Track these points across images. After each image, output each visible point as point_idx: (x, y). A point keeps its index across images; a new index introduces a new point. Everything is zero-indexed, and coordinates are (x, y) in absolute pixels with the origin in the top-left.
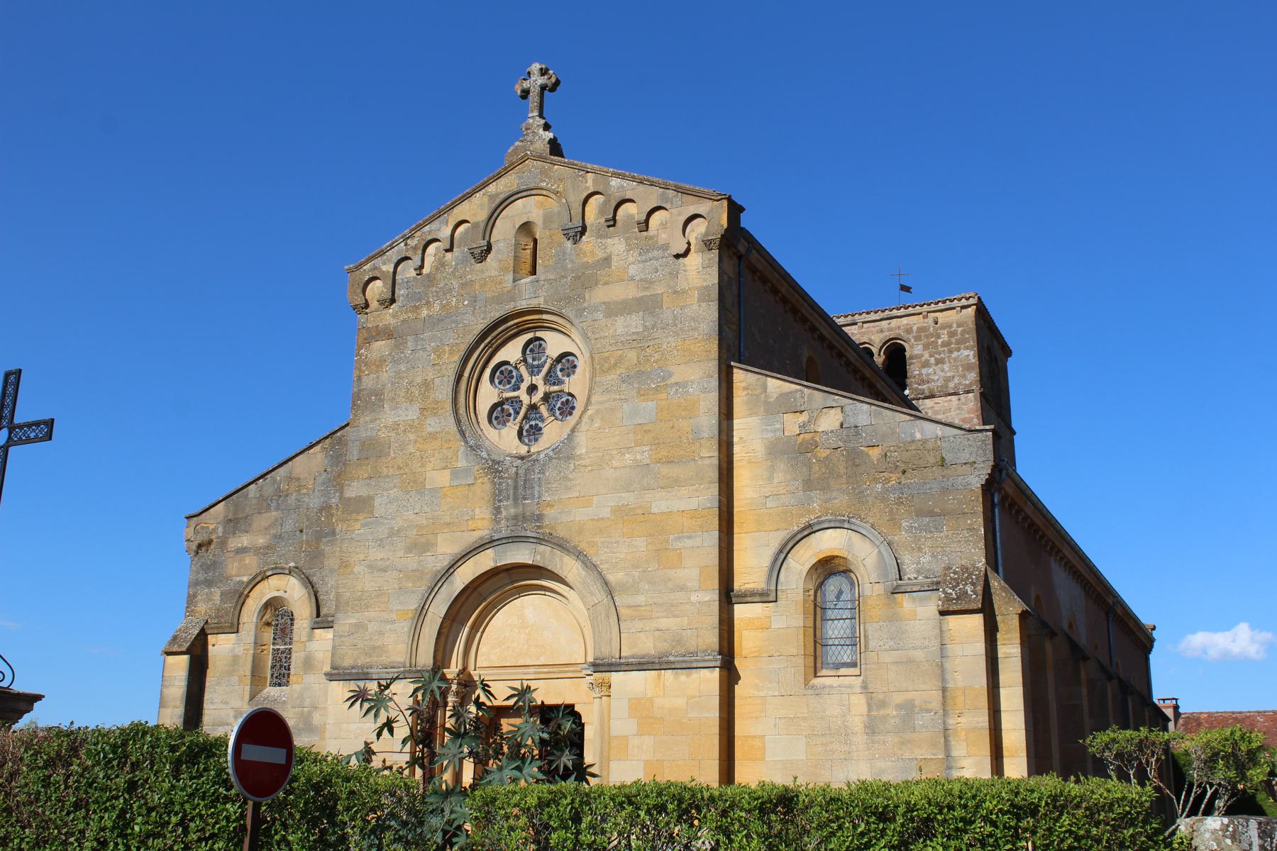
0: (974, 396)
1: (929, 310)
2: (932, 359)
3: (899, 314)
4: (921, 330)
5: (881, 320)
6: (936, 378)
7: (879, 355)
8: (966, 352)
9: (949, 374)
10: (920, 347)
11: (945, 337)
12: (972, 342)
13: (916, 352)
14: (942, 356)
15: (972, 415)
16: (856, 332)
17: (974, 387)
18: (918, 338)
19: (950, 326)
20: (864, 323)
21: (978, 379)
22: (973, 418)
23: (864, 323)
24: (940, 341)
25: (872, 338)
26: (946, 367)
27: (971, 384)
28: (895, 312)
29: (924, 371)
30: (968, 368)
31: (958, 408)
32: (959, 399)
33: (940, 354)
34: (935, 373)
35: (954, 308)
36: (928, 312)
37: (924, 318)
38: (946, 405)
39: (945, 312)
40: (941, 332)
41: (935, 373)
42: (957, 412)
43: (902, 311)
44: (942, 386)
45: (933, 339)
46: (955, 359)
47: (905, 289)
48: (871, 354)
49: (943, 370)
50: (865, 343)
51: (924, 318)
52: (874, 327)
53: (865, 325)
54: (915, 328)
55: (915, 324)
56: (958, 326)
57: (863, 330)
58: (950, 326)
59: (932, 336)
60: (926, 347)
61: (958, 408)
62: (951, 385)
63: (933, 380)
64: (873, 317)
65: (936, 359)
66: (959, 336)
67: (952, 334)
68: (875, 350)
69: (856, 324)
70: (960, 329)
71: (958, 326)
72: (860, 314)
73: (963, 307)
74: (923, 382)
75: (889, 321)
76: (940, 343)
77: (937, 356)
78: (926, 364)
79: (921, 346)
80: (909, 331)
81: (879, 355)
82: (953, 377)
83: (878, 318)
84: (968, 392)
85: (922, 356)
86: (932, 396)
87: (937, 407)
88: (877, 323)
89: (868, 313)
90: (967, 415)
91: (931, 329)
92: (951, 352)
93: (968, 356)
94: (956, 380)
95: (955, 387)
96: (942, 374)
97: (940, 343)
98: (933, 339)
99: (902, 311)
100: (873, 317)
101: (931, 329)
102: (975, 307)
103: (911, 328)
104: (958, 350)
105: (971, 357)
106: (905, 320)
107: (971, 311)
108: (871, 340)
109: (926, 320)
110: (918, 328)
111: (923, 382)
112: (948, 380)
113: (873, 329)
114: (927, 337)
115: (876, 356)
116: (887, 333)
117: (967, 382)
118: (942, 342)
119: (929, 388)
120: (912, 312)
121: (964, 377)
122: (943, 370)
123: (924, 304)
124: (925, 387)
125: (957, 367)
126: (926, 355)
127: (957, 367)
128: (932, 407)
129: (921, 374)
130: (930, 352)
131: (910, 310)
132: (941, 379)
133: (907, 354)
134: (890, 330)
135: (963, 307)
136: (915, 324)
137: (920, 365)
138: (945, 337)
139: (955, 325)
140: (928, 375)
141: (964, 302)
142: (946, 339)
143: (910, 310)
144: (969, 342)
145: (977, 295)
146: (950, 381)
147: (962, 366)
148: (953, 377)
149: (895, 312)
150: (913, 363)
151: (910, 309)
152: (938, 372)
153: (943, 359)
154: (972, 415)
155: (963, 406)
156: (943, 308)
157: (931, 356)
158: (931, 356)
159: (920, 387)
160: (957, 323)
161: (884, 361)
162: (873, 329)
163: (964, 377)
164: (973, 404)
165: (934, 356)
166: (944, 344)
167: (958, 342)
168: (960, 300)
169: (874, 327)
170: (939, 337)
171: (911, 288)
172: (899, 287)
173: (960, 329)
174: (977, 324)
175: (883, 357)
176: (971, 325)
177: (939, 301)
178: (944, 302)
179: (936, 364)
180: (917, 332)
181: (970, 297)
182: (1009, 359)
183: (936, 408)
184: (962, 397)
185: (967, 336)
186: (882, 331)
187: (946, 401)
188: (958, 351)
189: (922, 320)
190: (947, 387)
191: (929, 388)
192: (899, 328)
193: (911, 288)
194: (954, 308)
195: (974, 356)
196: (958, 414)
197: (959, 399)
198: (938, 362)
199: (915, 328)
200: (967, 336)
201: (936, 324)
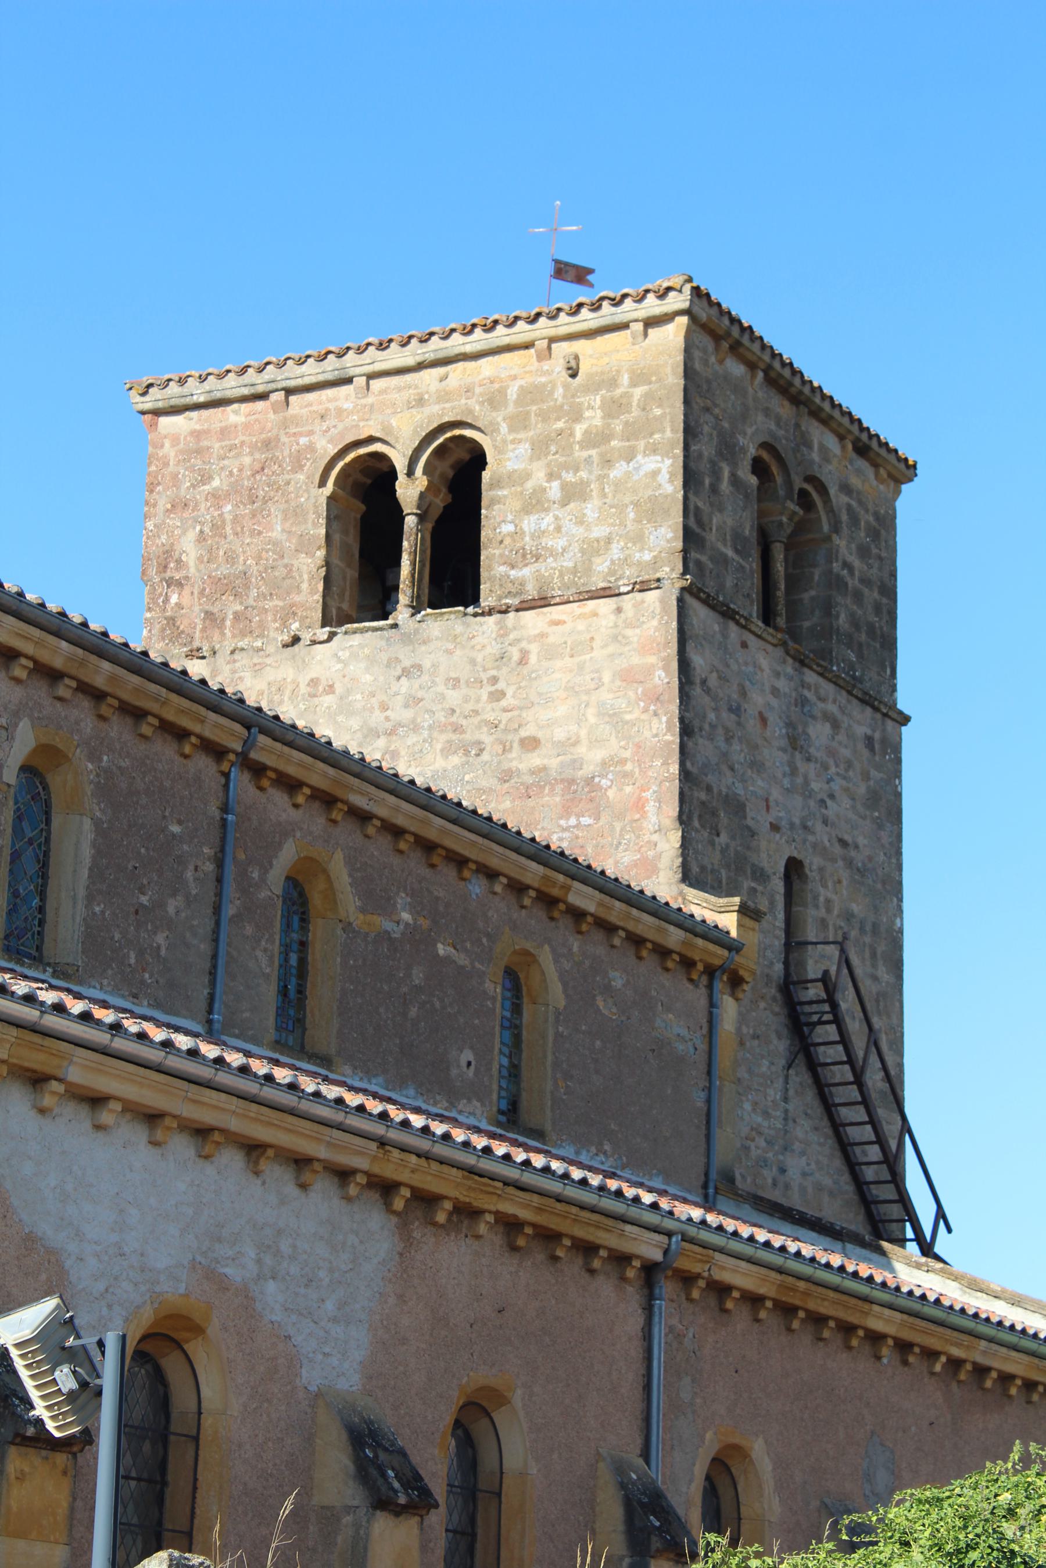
0: (662, 601)
1: (552, 332)
2: (556, 484)
3: (468, 349)
4: (532, 394)
5: (420, 367)
6: (560, 543)
7: (410, 473)
8: (649, 463)
9: (599, 532)
10: (524, 449)
11: (594, 418)
12: (672, 433)
13: (510, 466)
14: (583, 474)
15: (652, 659)
16: (348, 405)
17: (664, 572)
18: (519, 422)
19: (613, 383)
20: (371, 376)
21: (679, 545)
22: (650, 670)
23: (371, 376)
24: (579, 430)
25: (394, 422)
26: (591, 509)
27: (655, 562)
28: (458, 343)
29: (529, 524)
30: (651, 511)
31: (615, 638)
32: (619, 610)
33: (577, 470)
34: (558, 529)
35: (625, 326)
36: (552, 340)
37: (540, 358)
38: (581, 626)
39: (600, 341)
40: (583, 399)
41: (558, 529)
42: (611, 649)
43: (479, 340)
44: (574, 571)
45: (560, 425)
46: (618, 485)
47: (580, 275)
48: (393, 474)
49: (580, 521)
50: (371, 440)
51: (540, 358)
52: (399, 389)
53: (376, 384)
54: (512, 392)
55: (514, 378)
56: (634, 384)
57: (370, 400)
58: (613, 383)
59: (558, 411)
60: (540, 448)
61: (615, 638)
62: (601, 565)
63: (552, 552)
64: (396, 357)
65: (564, 486)
66: (635, 412)
67: (615, 407)
68: (400, 464)
69: (349, 381)
70: (638, 392)
71: (634, 384)
72: (360, 350)
73: (651, 322)
74: (523, 557)
75: (441, 371)
76: (578, 436)
77: (569, 477)
78: (535, 503)
79: (527, 446)
80: (495, 400)
81: (410, 473)
82: (609, 541)
83: (411, 361)
84: (644, 587)
85: (527, 475)
86: (542, 602)
87: (555, 636)
88: (409, 378)
89: (382, 346)
90: (636, 660)
91: (559, 392)
92: (607, 462)
93: (655, 473)
94: (615, 552)
95: (612, 572)
96: (579, 531)
97: (578, 436)
98: (560, 425)
99: (479, 340)
100: (396, 357)
101: (559, 392)
102: (684, 320)
103: (503, 392)
104: (629, 456)
105: (664, 477)
106: (487, 366)
107: (675, 333)
108: (388, 429)
109: (546, 366)
110: (524, 392)
111: (523, 557)
112: (593, 549)
113: (395, 396)
114: (544, 417)
115: (402, 477)
116: (436, 409)
117: (647, 556)
118: (587, 432)
119: (538, 577)
120: (506, 341)
121: (639, 539)
122: (580, 521)
123: (538, 315)
124: (526, 572)
125: (621, 508)
126: (539, 475)
127: (621, 508)
128: (543, 635)
129: (518, 533)
130: (548, 465)
131: (501, 335)
132: (575, 547)
133: (486, 475)
134: (444, 397)
135: (651, 322)
136: (514, 378)
137: (517, 505)
138: (594, 418)
139: (625, 379)
140: (542, 533)
141: (652, 306)
142: (598, 422)
143: (501, 335)
144: (662, 431)
145: (690, 280)
146: (597, 553)
147: (636, 504)
148: (609, 541)
149: (458, 343)
150: (493, 502)
151: (500, 330)
152: (568, 525)
153: (584, 484)
154: (652, 659)
155: (629, 632)
156: (593, 324)
157: (551, 476)
158: (551, 476)
159: (513, 573)
160: (632, 372)
161: (422, 496)
162: (395, 396)
163: (639, 539)
164: (655, 623)
165: (560, 477)
166: (596, 439)
167: (632, 432)
168: (640, 299)
169: (399, 389)
170: (577, 416)
171: (591, 271)
172: (550, 268)
173: (638, 392)
174: (689, 372)
175: (421, 481)
176: (674, 380)
177: (580, 305)
178: (596, 307)
179: (564, 504)
180: (520, 401)
181: (669, 289)
182: (904, 487)
183: (551, 639)
184: (627, 602)
185: (658, 412)
186: (420, 402)
187: (582, 616)
188: (629, 460)
189: (534, 364)
190: (588, 570)
191: (538, 577)
192: (469, 390)
193: (591, 271)
194: (625, 326)
195: (672, 474)
196: (612, 656)
197: (619, 610)
198: (573, 494)
199: (512, 392)
200: (658, 412)
201: (574, 376)
